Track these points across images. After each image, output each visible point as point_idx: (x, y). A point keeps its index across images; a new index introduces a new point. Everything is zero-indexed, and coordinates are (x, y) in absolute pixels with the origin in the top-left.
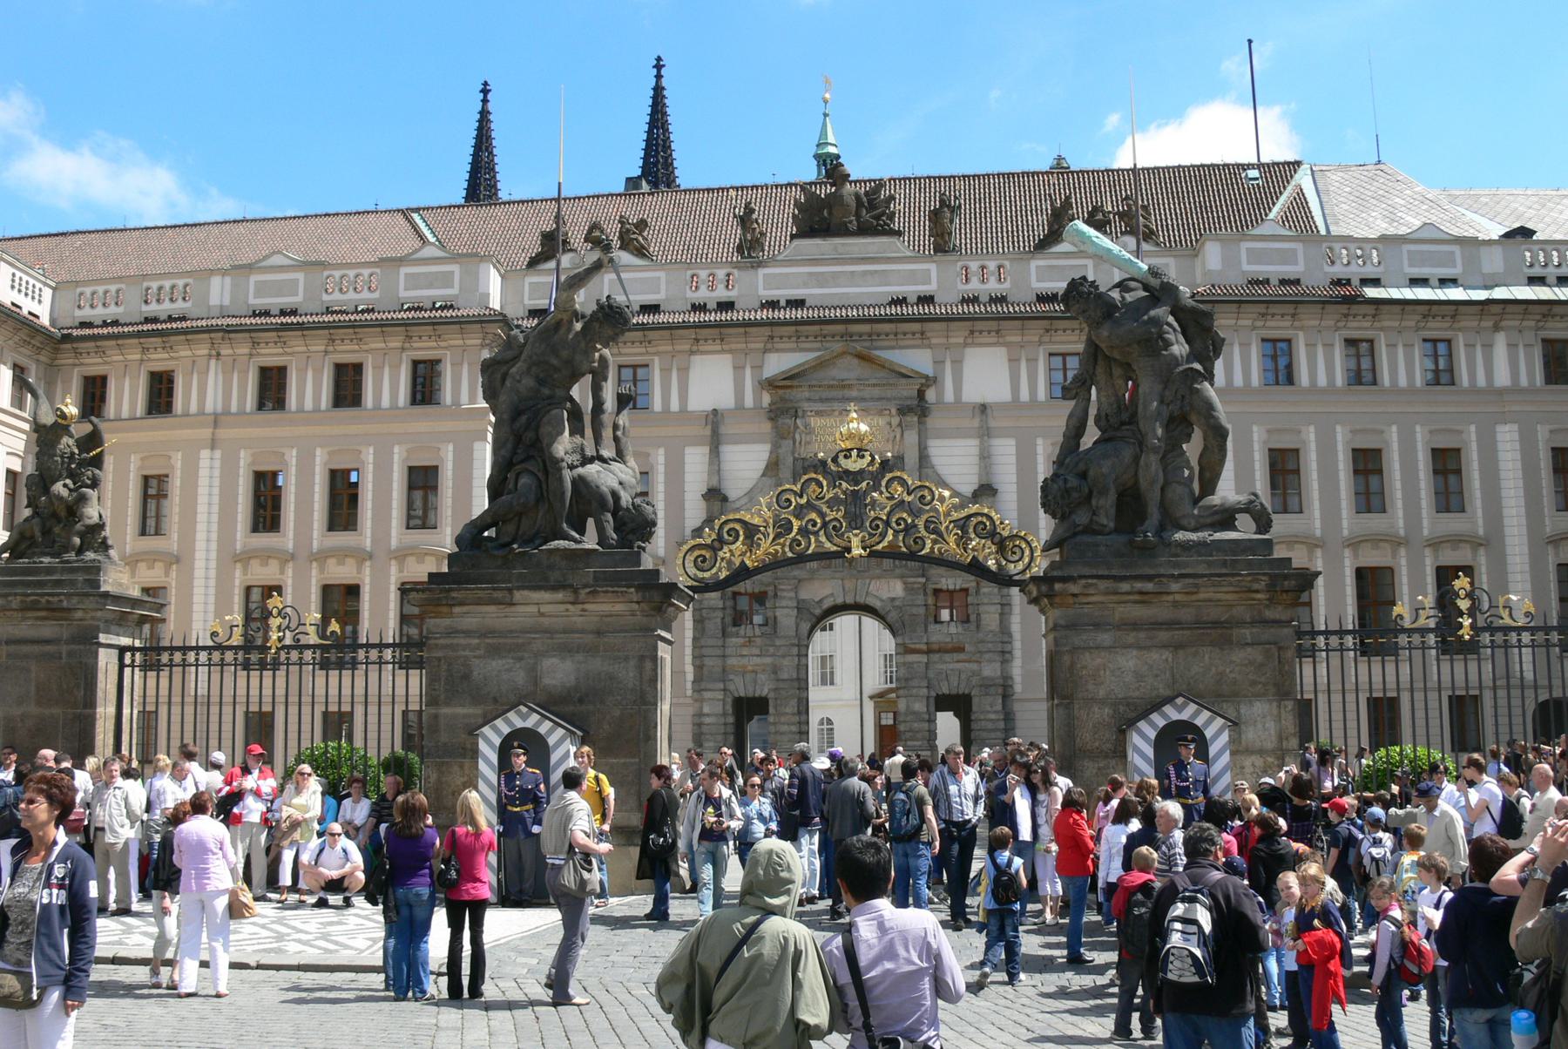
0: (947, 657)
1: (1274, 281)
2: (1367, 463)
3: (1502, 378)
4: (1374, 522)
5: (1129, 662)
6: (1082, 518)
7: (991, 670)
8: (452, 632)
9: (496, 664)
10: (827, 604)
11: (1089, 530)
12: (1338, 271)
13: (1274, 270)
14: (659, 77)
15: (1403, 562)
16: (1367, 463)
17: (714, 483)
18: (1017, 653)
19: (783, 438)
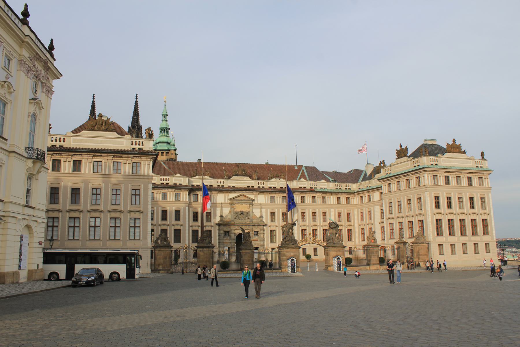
0: (256, 241)
1: (303, 188)
2: (314, 214)
3: (332, 203)
4: (315, 223)
5: (333, 253)
6: (329, 241)
7: (262, 243)
8: (284, 251)
9: (287, 254)
10: (238, 233)
11: (330, 242)
12: (311, 186)
13: (303, 186)
14: (137, 98)
15: (319, 229)
16: (314, 214)
17: (222, 214)
18: (265, 241)
19: (232, 208)
